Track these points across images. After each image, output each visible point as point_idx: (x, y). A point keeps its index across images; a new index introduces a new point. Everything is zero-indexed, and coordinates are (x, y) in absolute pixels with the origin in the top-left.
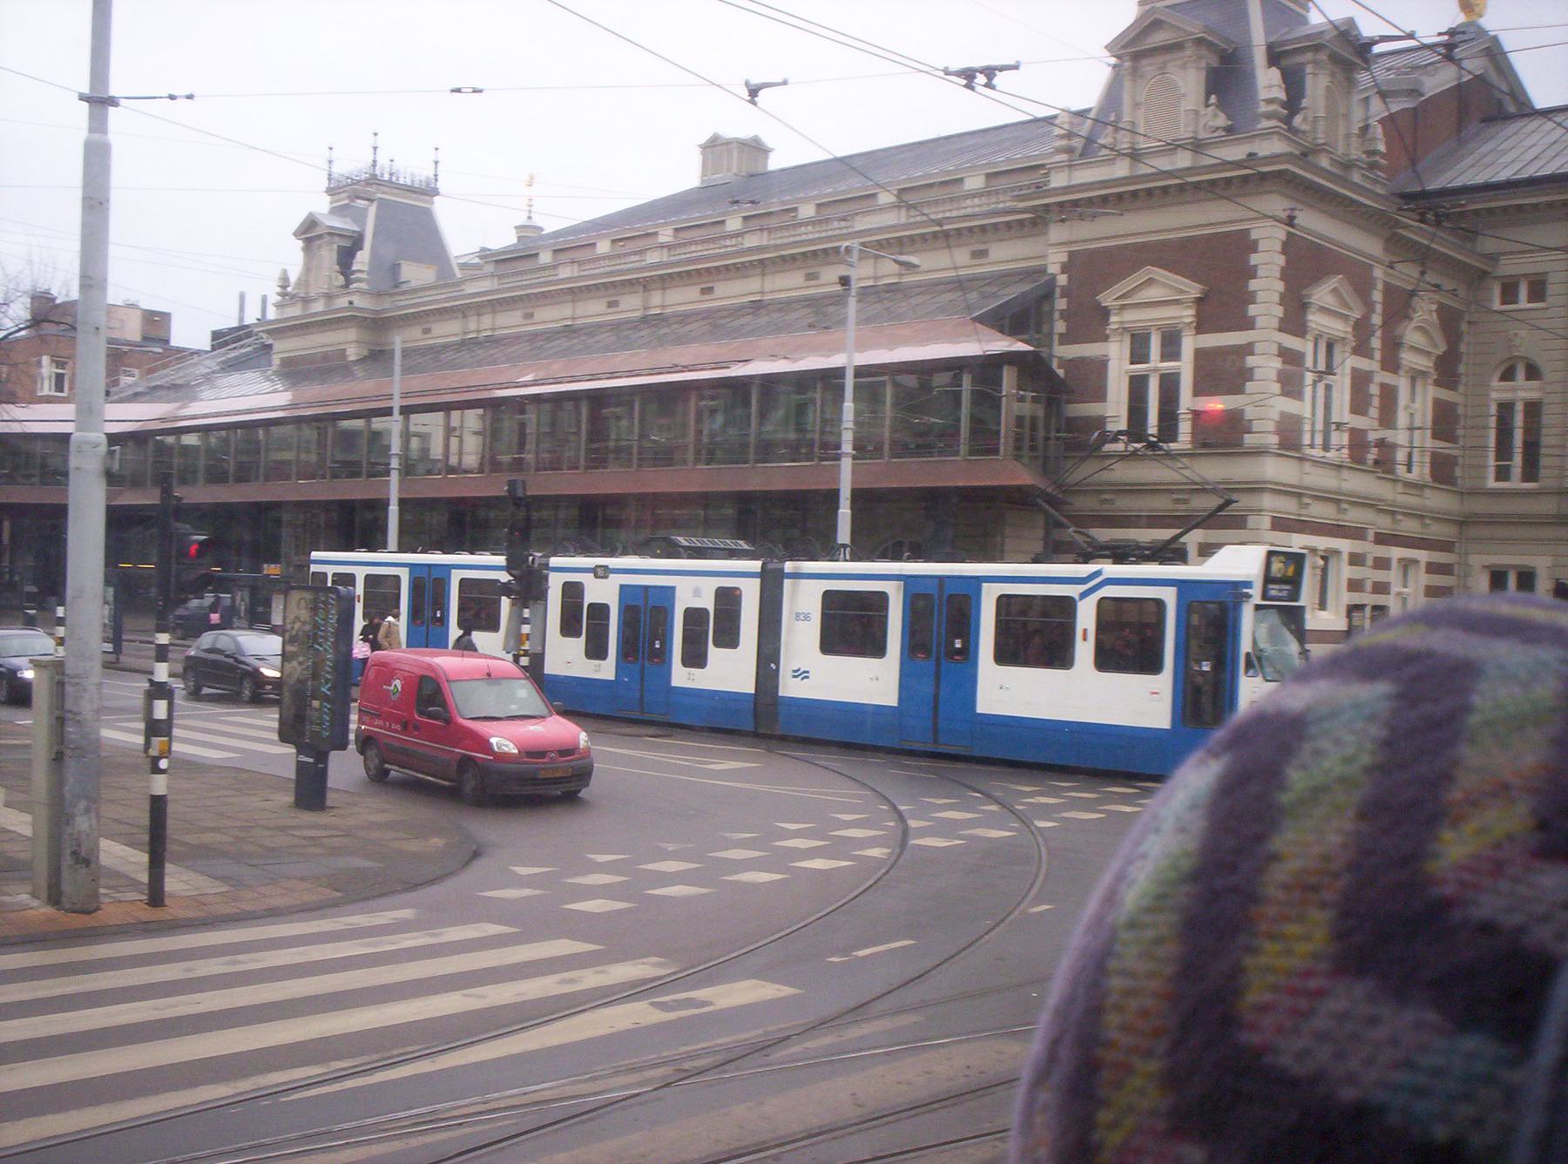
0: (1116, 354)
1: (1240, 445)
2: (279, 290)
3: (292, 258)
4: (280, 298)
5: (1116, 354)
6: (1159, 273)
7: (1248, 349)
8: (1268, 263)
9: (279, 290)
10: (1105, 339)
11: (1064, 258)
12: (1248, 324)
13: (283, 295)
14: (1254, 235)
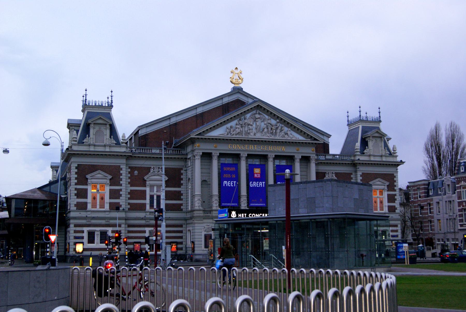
1: (395, 212)
6: (379, 179)
11: (361, 174)
14: (395, 175)
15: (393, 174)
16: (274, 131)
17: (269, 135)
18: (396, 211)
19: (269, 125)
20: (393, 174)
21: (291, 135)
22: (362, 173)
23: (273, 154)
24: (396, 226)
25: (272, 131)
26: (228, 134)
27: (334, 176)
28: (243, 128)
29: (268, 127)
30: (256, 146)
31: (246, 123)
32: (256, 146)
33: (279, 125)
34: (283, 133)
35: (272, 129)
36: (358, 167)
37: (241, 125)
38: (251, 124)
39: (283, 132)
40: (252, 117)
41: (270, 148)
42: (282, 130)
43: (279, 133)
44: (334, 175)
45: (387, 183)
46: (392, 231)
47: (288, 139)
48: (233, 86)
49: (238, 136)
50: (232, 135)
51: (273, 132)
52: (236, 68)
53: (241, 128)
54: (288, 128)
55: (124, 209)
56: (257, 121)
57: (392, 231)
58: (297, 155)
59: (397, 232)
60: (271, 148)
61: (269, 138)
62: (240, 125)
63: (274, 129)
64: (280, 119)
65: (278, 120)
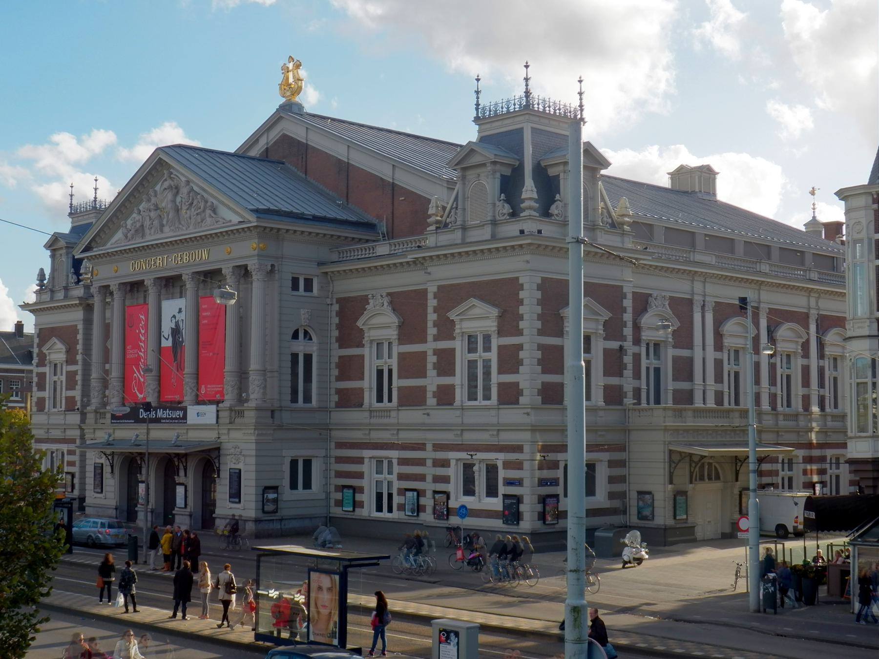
0: (459, 345)
1: (517, 402)
2: (38, 282)
3: (45, 261)
4: (39, 288)
5: (459, 345)
7: (520, 347)
8: (529, 296)
9: (38, 282)
10: (454, 338)
12: (520, 333)
13: (41, 285)
15: (517, 279)
18: (522, 400)
20: (517, 279)
22: (439, 287)
24: (518, 449)
27: (386, 304)
36: (429, 270)
44: (386, 301)
45: (494, 312)
46: (507, 465)
48: (284, 100)
52: (291, 59)
55: (78, 409)
57: (507, 465)
59: (522, 469)
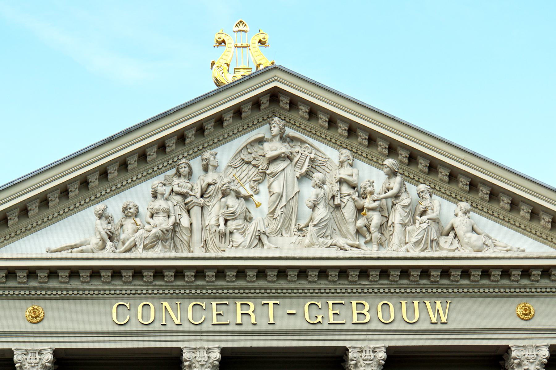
16: (376, 219)
17: (341, 241)
19: (345, 189)
21: (474, 235)
23: (373, 344)
25: (361, 222)
26: (103, 247)
28: (196, 211)
29: (337, 201)
30: (271, 303)
31: (211, 187)
32: (271, 303)
33: (402, 185)
34: (424, 226)
35: (360, 210)
37: (184, 196)
38: (245, 190)
39: (424, 218)
40: (249, 158)
41: (355, 312)
42: (423, 213)
43: (404, 225)
47: (456, 254)
49: (157, 252)
50: (129, 250)
51: (367, 227)
53: (185, 215)
54: (456, 200)
56: (274, 175)
58: (521, 343)
60: (364, 312)
61: (342, 254)
62: (178, 198)
63: (374, 209)
64: (403, 155)
65: (390, 162)
